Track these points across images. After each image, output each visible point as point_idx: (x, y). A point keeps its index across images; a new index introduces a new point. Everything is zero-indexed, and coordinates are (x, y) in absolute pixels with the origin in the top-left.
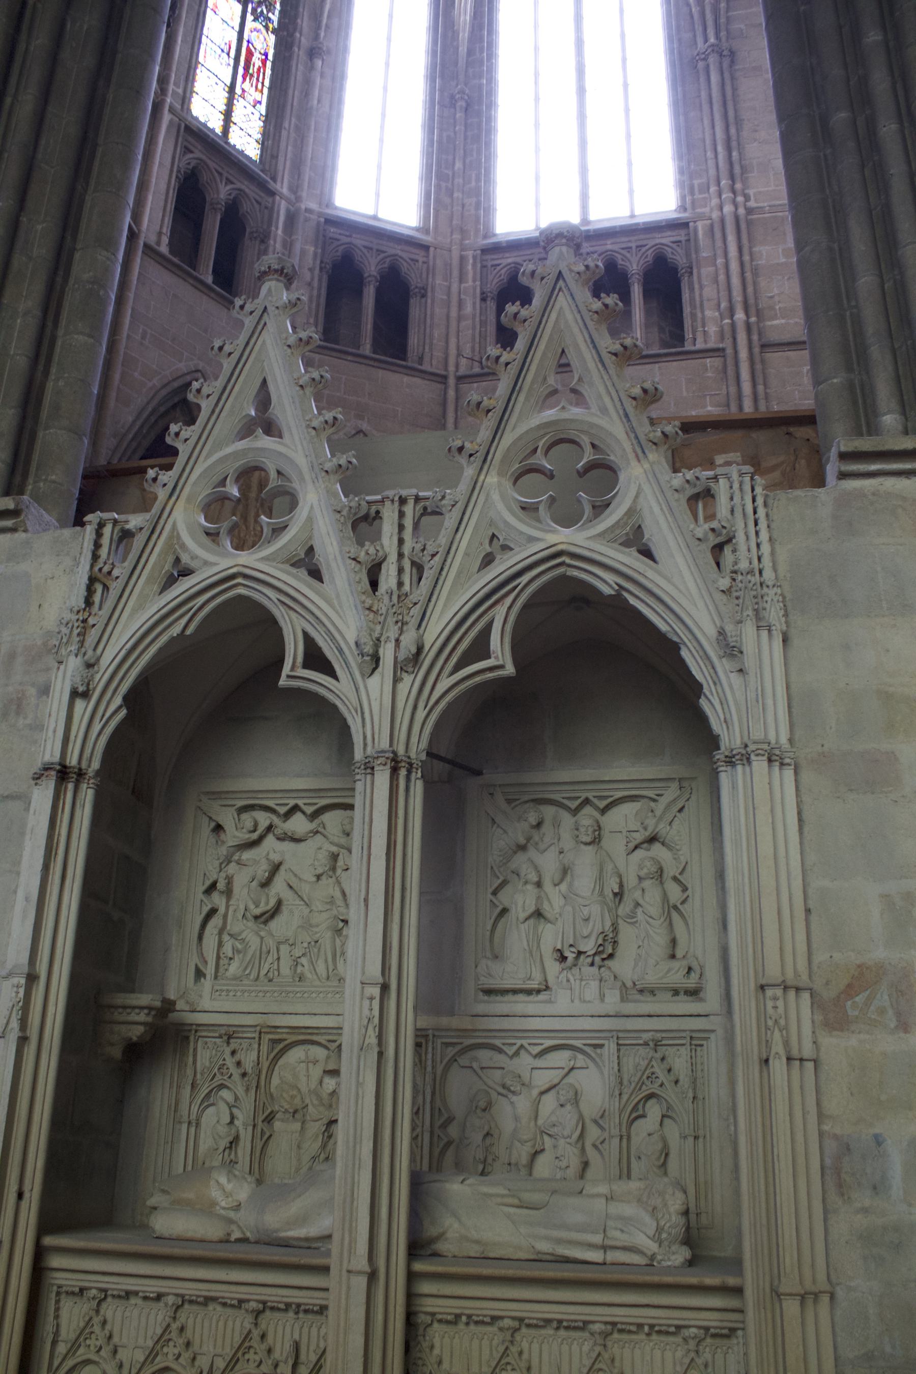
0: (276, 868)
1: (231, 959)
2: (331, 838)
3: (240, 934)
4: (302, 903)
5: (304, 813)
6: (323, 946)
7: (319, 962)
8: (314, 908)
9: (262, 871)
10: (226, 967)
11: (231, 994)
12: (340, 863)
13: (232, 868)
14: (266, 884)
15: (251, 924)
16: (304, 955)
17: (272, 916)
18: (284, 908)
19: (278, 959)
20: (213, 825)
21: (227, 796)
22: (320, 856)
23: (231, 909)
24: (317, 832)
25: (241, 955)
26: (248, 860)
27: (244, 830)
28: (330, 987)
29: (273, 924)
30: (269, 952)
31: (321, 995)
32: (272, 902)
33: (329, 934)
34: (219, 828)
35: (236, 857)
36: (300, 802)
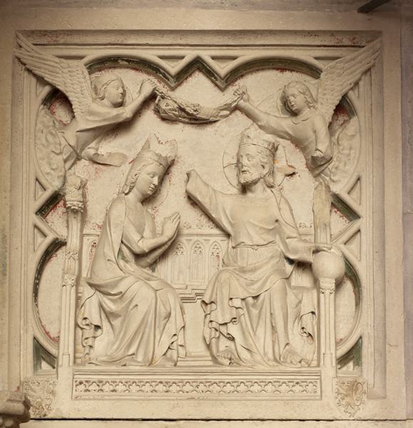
0: (167, 169)
1: (97, 327)
2: (264, 119)
3: (115, 284)
4: (216, 231)
5: (210, 73)
6: (267, 305)
7: (260, 332)
8: (243, 239)
9: (146, 176)
10: (90, 342)
11: (107, 388)
12: (281, 163)
13: (83, 169)
14: (147, 200)
15: (132, 266)
16: (234, 320)
17: (164, 256)
18: (183, 239)
19: (184, 327)
20: (47, 89)
21: (69, 39)
22: (252, 150)
23: (87, 242)
24: (237, 108)
25: (116, 322)
26: (110, 155)
27: (105, 101)
28: (285, 373)
29: (166, 269)
30: (169, 315)
31: (269, 388)
32: (169, 232)
33: (276, 283)
34: (57, 97)
35: (90, 151)
36: (206, 55)
